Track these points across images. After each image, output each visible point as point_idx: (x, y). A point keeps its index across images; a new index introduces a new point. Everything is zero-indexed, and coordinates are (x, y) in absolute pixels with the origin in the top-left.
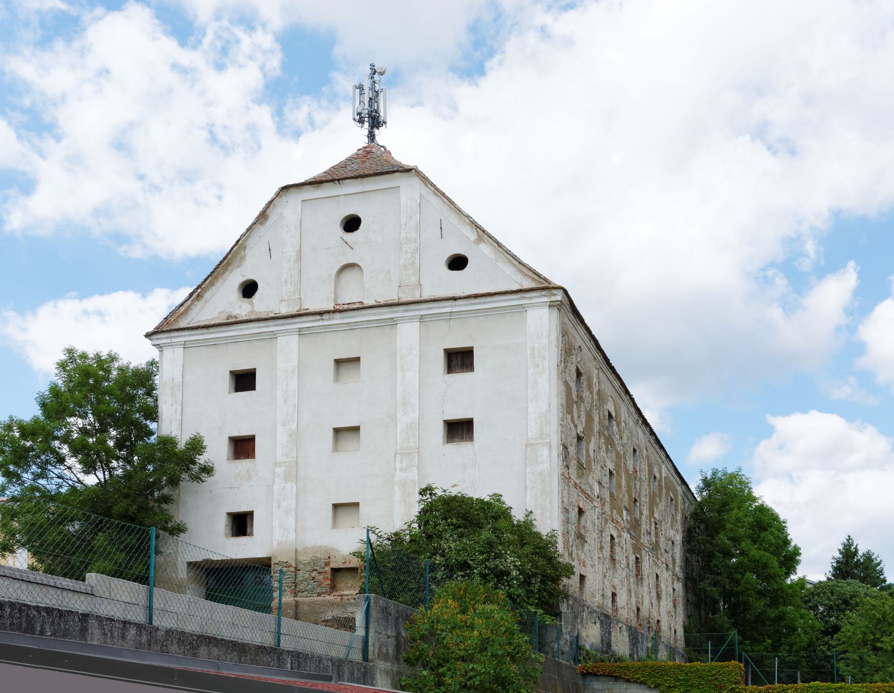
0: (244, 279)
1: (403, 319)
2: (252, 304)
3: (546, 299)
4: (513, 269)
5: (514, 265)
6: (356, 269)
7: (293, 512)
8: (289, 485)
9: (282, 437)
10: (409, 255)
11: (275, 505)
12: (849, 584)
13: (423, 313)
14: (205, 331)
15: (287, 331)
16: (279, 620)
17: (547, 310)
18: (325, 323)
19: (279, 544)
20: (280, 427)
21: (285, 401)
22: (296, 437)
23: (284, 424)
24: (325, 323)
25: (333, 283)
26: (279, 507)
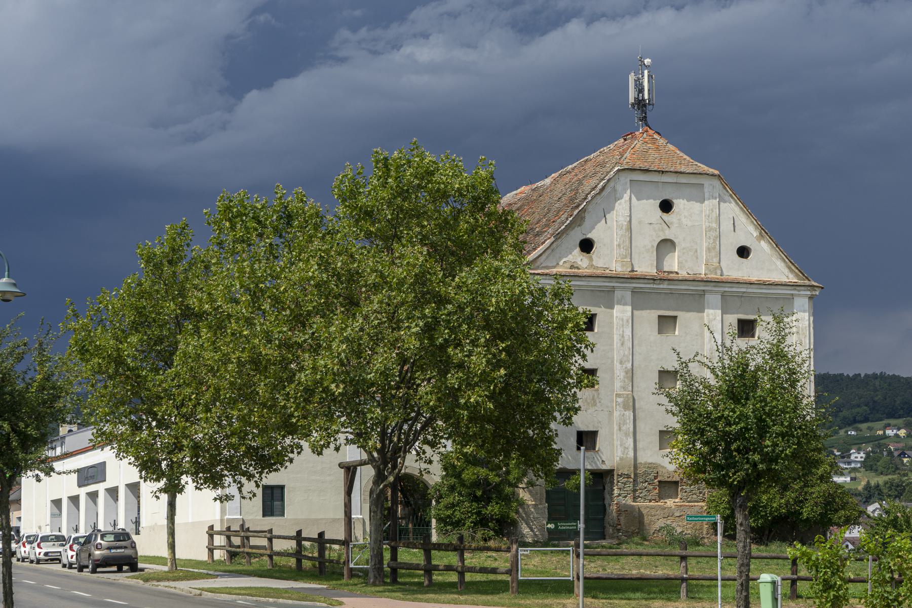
0: (584, 237)
1: (711, 291)
2: (591, 259)
3: (809, 293)
4: (783, 264)
5: (784, 261)
6: (669, 244)
7: (631, 435)
8: (627, 413)
9: (619, 372)
10: (712, 241)
11: (616, 428)
12: (773, 552)
13: (726, 289)
14: (608, 280)
15: (624, 288)
16: (172, 546)
17: (807, 300)
18: (655, 286)
19: (621, 459)
20: (617, 365)
21: (622, 344)
22: (631, 374)
23: (621, 363)
24: (655, 286)
25: (655, 253)
26: (620, 429)
